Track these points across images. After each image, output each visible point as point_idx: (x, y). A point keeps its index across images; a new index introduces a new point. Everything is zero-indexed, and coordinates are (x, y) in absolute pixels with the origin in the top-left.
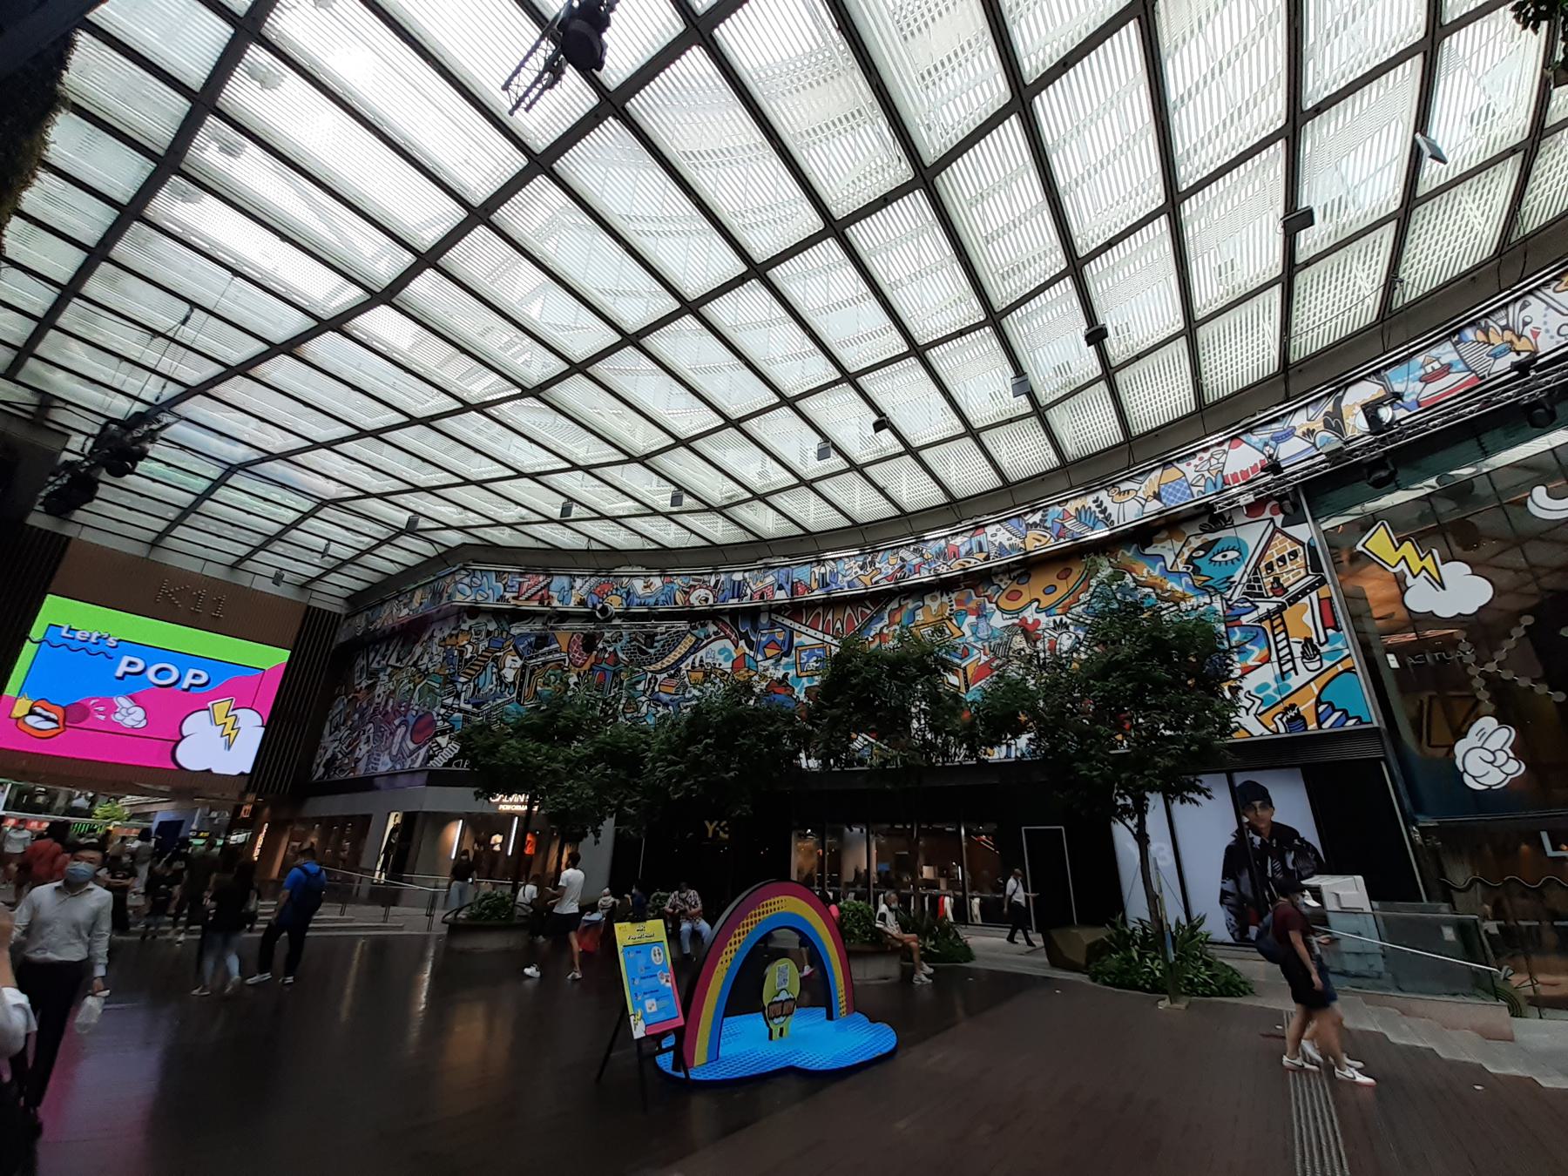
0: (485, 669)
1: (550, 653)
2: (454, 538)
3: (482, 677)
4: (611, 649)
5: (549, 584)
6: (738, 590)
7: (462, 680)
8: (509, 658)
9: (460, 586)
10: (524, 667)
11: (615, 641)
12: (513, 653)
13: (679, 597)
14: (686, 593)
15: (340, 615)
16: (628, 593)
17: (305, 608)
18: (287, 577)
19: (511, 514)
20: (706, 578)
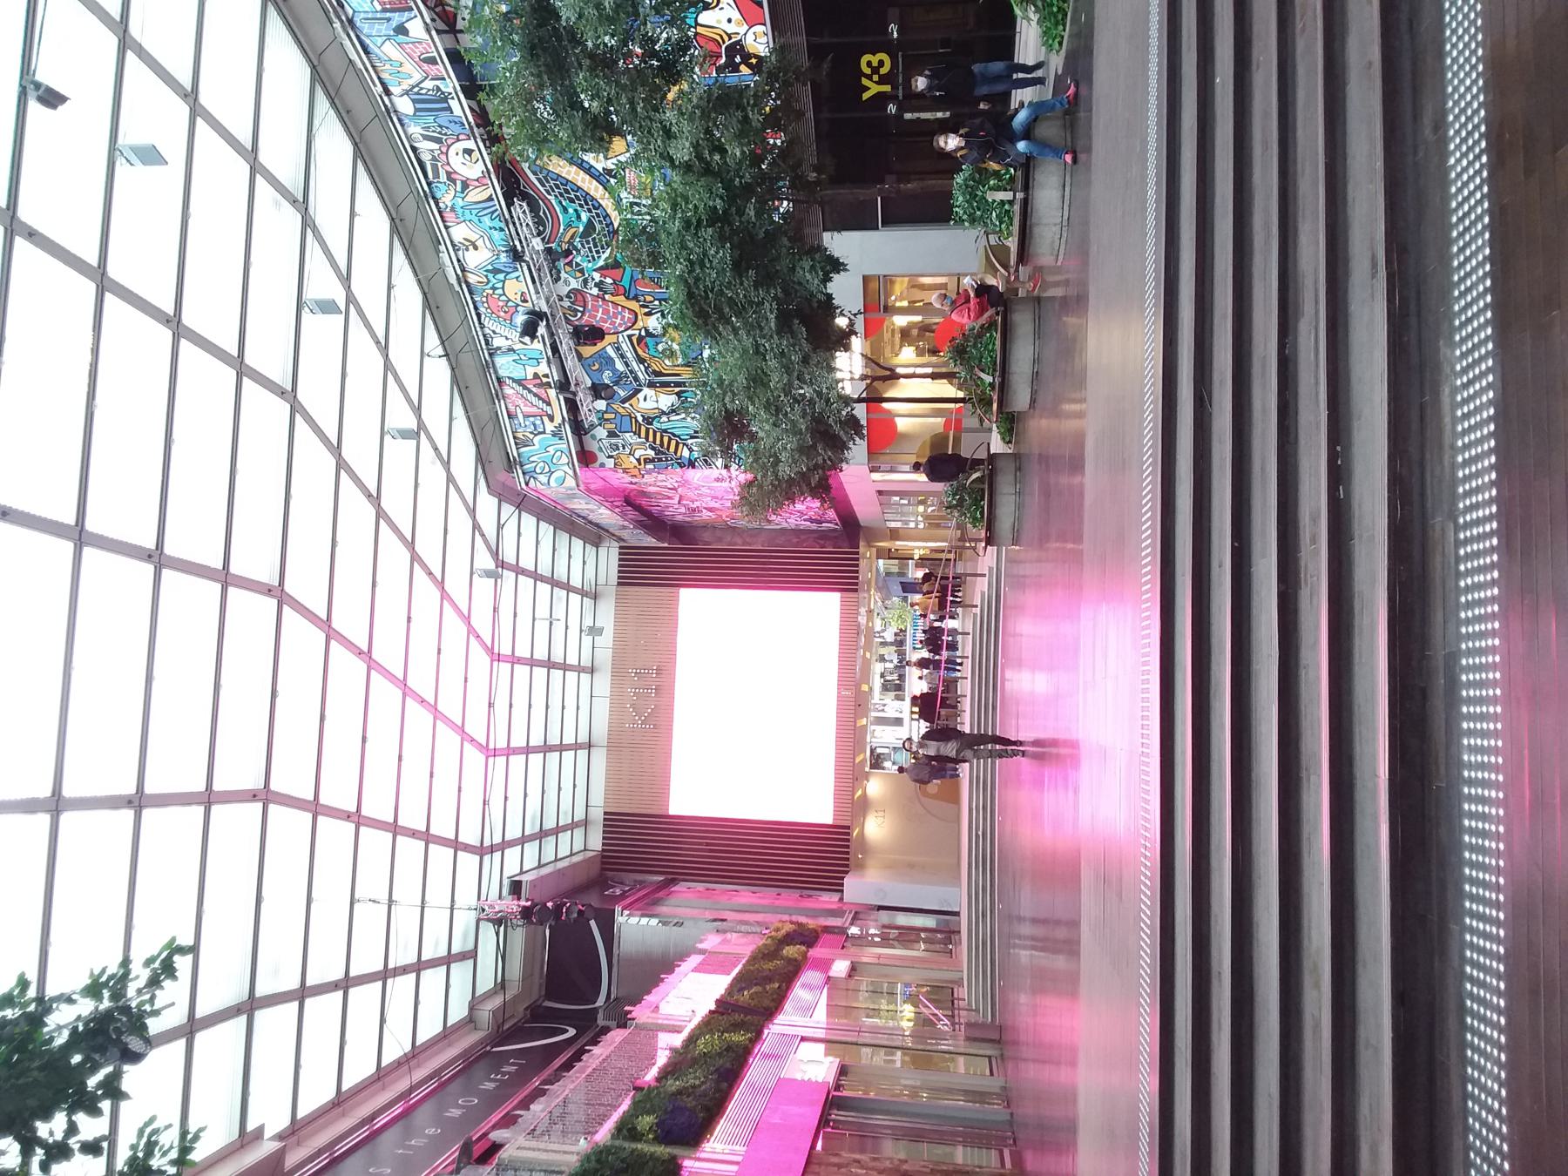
0: (665, 431)
1: (622, 356)
2: (487, 504)
3: (676, 432)
4: (597, 276)
5: (514, 381)
6: (432, 103)
7: (686, 453)
8: (643, 405)
9: (553, 483)
10: (651, 385)
11: (582, 271)
12: (633, 401)
13: (475, 195)
14: (465, 185)
15: (621, 548)
16: (496, 271)
17: (621, 588)
18: (588, 622)
19: (433, 474)
20: (426, 157)
